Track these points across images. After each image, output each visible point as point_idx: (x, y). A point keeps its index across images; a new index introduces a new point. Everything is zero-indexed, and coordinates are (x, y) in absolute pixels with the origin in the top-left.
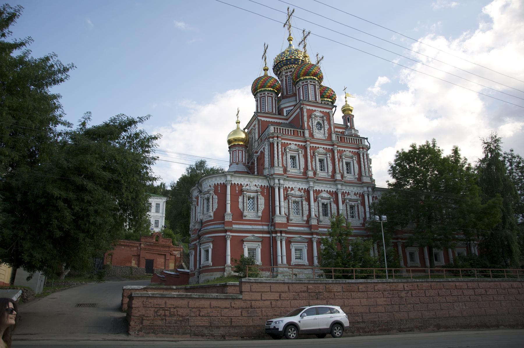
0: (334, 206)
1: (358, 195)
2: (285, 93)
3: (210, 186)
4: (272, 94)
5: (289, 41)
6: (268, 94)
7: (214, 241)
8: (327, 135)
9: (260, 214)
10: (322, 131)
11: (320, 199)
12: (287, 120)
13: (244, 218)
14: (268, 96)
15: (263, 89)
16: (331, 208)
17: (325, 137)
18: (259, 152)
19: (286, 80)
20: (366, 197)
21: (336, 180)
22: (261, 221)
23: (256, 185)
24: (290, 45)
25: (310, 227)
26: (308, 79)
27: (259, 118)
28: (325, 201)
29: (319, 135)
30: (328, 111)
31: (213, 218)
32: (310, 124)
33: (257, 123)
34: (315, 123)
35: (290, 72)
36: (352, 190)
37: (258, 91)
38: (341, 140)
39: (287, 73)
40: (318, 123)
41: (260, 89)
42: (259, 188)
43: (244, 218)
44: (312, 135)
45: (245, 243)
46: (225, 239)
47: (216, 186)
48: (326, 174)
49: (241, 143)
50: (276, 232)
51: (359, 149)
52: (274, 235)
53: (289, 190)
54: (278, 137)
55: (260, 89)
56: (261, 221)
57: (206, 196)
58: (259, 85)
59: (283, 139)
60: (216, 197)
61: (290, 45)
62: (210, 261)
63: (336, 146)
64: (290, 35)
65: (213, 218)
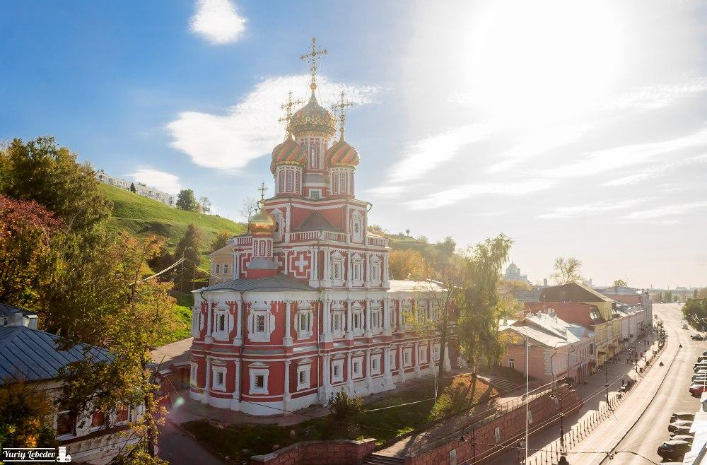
3: (265, 302)
8: (363, 239)
9: (312, 333)
24: (313, 96)
27: (293, 204)
29: (357, 237)
30: (363, 209)
31: (269, 341)
34: (354, 223)
37: (286, 162)
46: (283, 363)
47: (273, 304)
50: (323, 352)
56: (311, 340)
58: (289, 157)
60: (273, 318)
61: (313, 96)
62: (264, 390)
65: (269, 341)
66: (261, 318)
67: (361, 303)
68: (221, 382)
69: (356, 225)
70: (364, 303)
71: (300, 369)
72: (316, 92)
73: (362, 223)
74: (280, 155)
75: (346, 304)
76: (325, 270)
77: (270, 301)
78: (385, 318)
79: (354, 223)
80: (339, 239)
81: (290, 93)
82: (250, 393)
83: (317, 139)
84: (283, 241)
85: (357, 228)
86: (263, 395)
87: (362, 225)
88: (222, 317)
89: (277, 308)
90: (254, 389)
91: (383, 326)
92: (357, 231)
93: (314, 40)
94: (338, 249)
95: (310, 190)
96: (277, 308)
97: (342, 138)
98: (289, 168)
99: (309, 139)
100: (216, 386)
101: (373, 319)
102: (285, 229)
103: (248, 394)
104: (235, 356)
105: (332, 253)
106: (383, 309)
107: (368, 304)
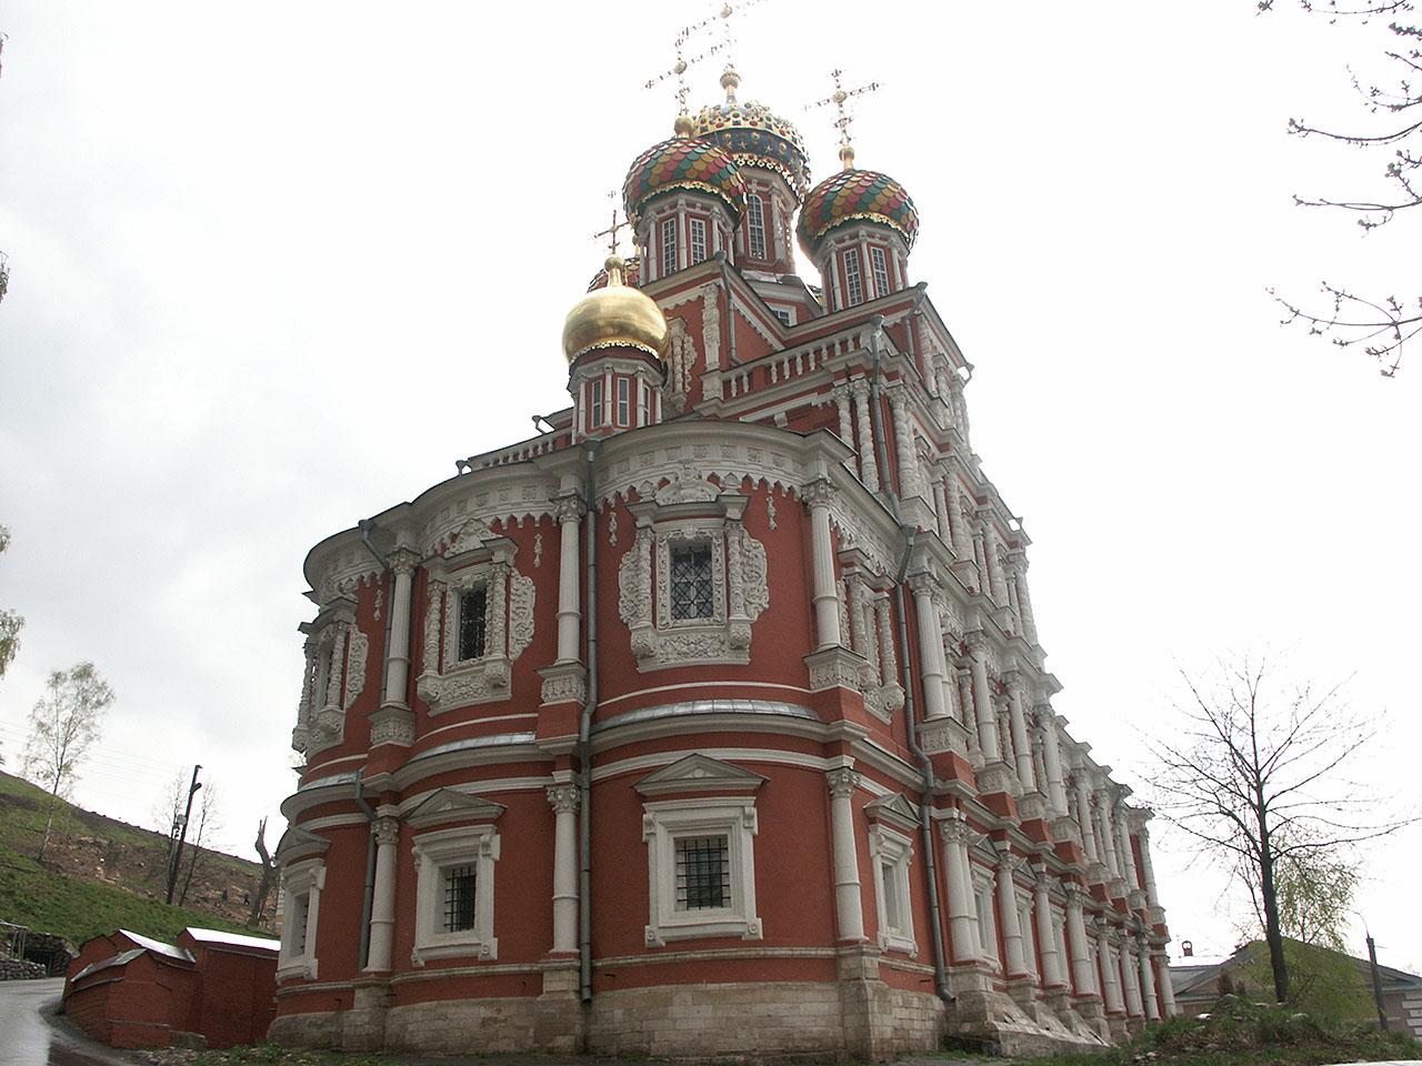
7: (768, 788)
33: (711, 300)
35: (758, 184)
37: (688, 186)
41: (699, 185)
45: (881, 828)
49: (655, 353)
52: (935, 813)
55: (699, 185)
57: (690, 530)
62: (742, 913)
65: (745, 660)
66: (693, 557)
68: (464, 916)
77: (740, 477)
82: (655, 932)
86: (734, 940)
88: (474, 603)
89: (772, 511)
90: (668, 914)
96: (772, 511)
100: (430, 934)
102: (699, 369)
103: (638, 945)
104: (546, 767)
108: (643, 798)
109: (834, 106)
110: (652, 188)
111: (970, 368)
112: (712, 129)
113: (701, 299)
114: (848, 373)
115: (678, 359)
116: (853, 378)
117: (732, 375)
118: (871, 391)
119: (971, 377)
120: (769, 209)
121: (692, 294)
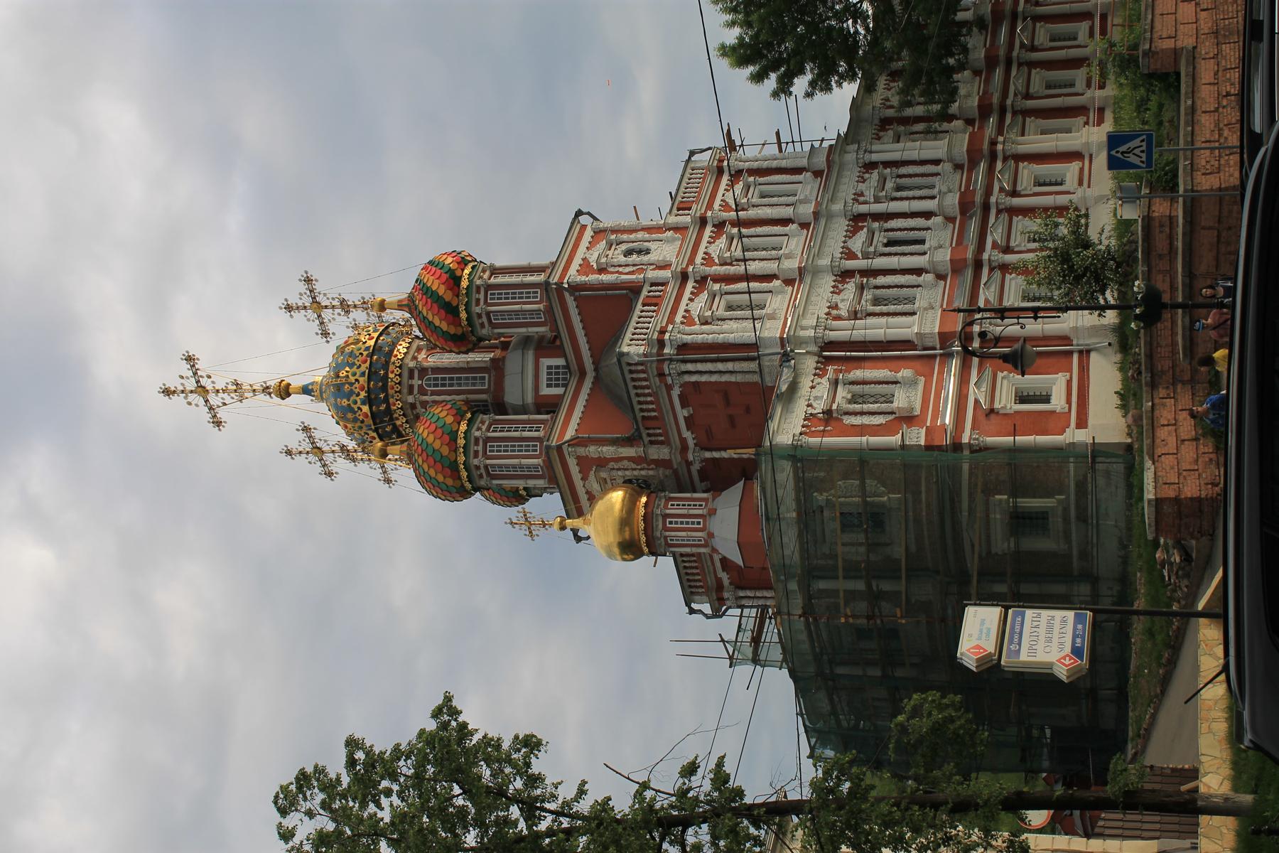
0: (893, 224)
1: (867, 176)
2: (484, 396)
4: (483, 423)
5: (289, 395)
6: (479, 429)
8: (670, 234)
9: (905, 373)
10: (652, 246)
11: (872, 249)
12: (583, 374)
13: (917, 412)
14: (488, 430)
15: (461, 442)
16: (900, 230)
17: (674, 240)
18: (687, 434)
19: (433, 393)
20: (875, 157)
21: (816, 215)
22: (929, 377)
23: (812, 387)
24: (306, 390)
25: (957, 267)
26: (471, 281)
28: (880, 238)
29: (666, 250)
30: (588, 234)
32: (628, 269)
33: (581, 451)
34: (622, 259)
35: (411, 377)
36: (848, 187)
37: (462, 459)
38: (655, 305)
39: (411, 388)
40: (628, 253)
42: (825, 381)
43: (917, 412)
44: (664, 266)
45: (997, 406)
48: (793, 242)
51: (720, 171)
53: (834, 312)
54: (663, 332)
59: (671, 320)
61: (306, 390)
63: (709, 214)
64: (266, 390)
67: (853, 231)
69: (628, 253)
70: (857, 220)
71: (1005, 400)
72: (296, 383)
73: (625, 237)
74: (440, 478)
75: (845, 275)
76: (731, 338)
78: (914, 155)
79: (622, 259)
80: (654, 302)
81: (289, 453)
83: (411, 377)
84: (664, 464)
85: (639, 252)
87: (632, 236)
91: (936, 162)
92: (648, 252)
93: (167, 392)
94: (685, 300)
95: (545, 391)
97: (400, 306)
98: (476, 453)
99: (410, 399)
101: (911, 193)
105: (688, 320)
106: (887, 164)
107: (863, 209)
108: (989, 552)
109: (327, 314)
110: (462, 486)
111: (579, 213)
112: (369, 421)
113: (578, 458)
114: (661, 375)
115: (627, 473)
116: (667, 372)
117: (646, 439)
118: (678, 361)
119: (589, 214)
120: (436, 370)
121: (572, 463)
